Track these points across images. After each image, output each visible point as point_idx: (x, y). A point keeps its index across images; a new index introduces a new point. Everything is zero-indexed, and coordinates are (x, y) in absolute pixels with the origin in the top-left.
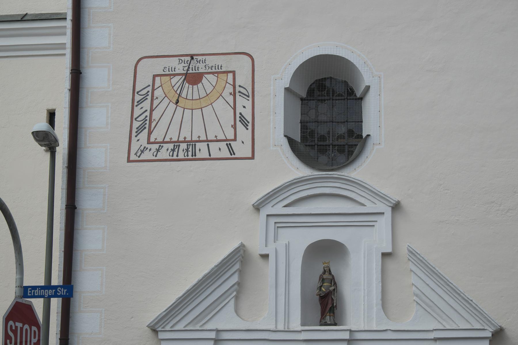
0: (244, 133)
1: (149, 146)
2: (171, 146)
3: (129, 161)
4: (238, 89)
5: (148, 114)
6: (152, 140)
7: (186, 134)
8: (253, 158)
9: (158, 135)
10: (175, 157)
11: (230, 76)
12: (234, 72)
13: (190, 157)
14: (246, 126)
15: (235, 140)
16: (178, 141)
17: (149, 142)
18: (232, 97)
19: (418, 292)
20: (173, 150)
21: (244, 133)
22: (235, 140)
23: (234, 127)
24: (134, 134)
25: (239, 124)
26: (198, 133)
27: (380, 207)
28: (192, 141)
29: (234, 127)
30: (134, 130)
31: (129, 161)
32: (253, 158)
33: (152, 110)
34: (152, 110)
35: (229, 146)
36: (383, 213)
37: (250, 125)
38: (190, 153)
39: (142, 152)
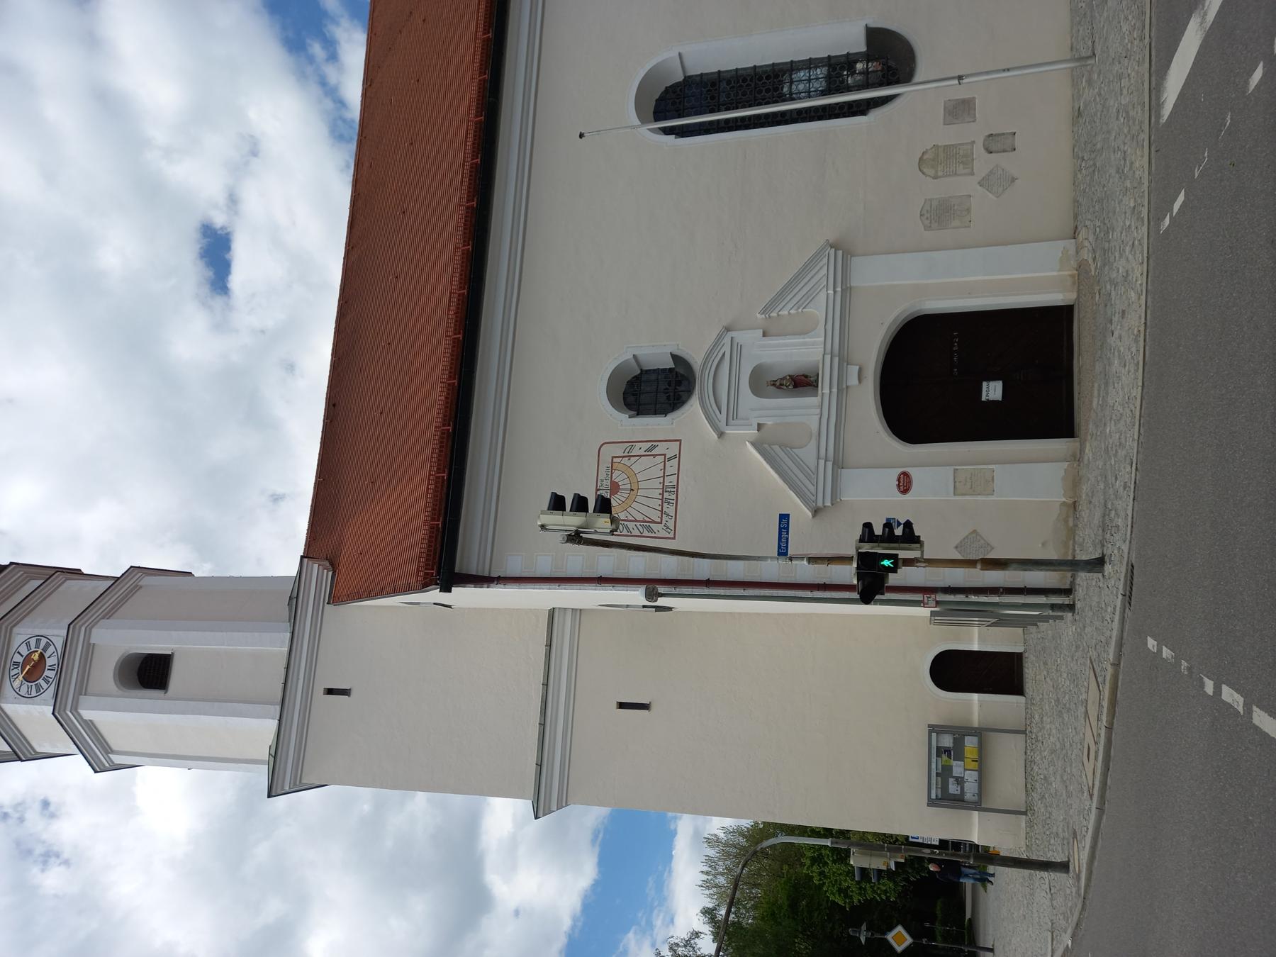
0: (661, 448)
1: (664, 522)
2: (665, 505)
3: (674, 538)
4: (626, 454)
5: (638, 524)
6: (659, 520)
7: (657, 494)
8: (680, 441)
9: (655, 516)
10: (674, 502)
11: (615, 460)
12: (613, 457)
13: (675, 490)
14: (655, 447)
15: (665, 455)
16: (662, 500)
17: (661, 523)
18: (632, 458)
19: (795, 308)
20: (669, 503)
21: (661, 448)
22: (665, 455)
23: (655, 456)
24: (653, 535)
25: (653, 453)
26: (657, 484)
27: (727, 340)
28: (663, 489)
29: (655, 456)
30: (650, 534)
31: (674, 538)
32: (680, 441)
33: (636, 521)
34: (636, 521)
35: (670, 459)
36: (732, 338)
37: (654, 444)
38: (672, 490)
39: (668, 528)
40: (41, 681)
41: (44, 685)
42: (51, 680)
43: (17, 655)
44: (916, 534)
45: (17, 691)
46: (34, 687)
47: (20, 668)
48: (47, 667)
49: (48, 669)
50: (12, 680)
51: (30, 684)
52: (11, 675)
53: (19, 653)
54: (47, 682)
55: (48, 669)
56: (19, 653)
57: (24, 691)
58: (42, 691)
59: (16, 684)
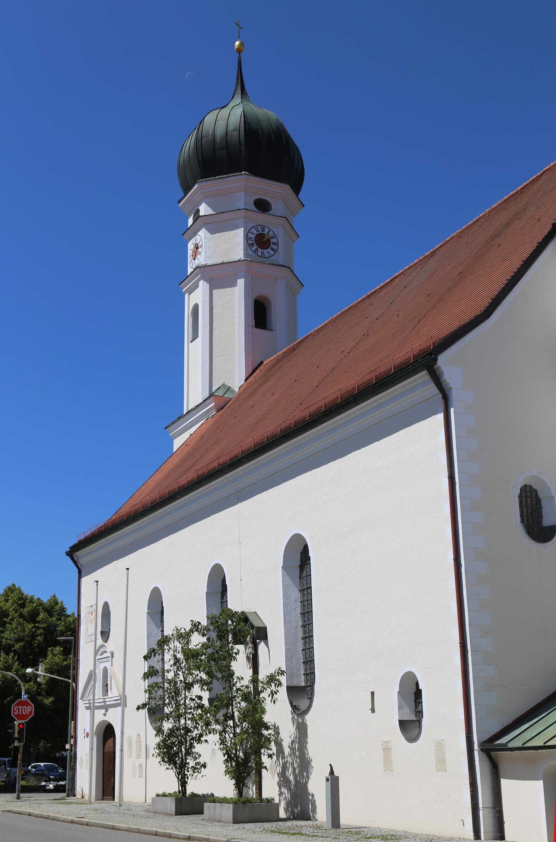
40: (256, 246)
41: (254, 249)
42: (256, 253)
43: (268, 230)
44: (420, 689)
45: (250, 231)
46: (252, 242)
47: (261, 232)
48: (263, 250)
49: (262, 251)
50: (255, 227)
51: (254, 239)
52: (258, 226)
53: (269, 231)
54: (255, 251)
55: (262, 251)
56: (269, 231)
57: (251, 235)
58: (251, 247)
59: (254, 231)
